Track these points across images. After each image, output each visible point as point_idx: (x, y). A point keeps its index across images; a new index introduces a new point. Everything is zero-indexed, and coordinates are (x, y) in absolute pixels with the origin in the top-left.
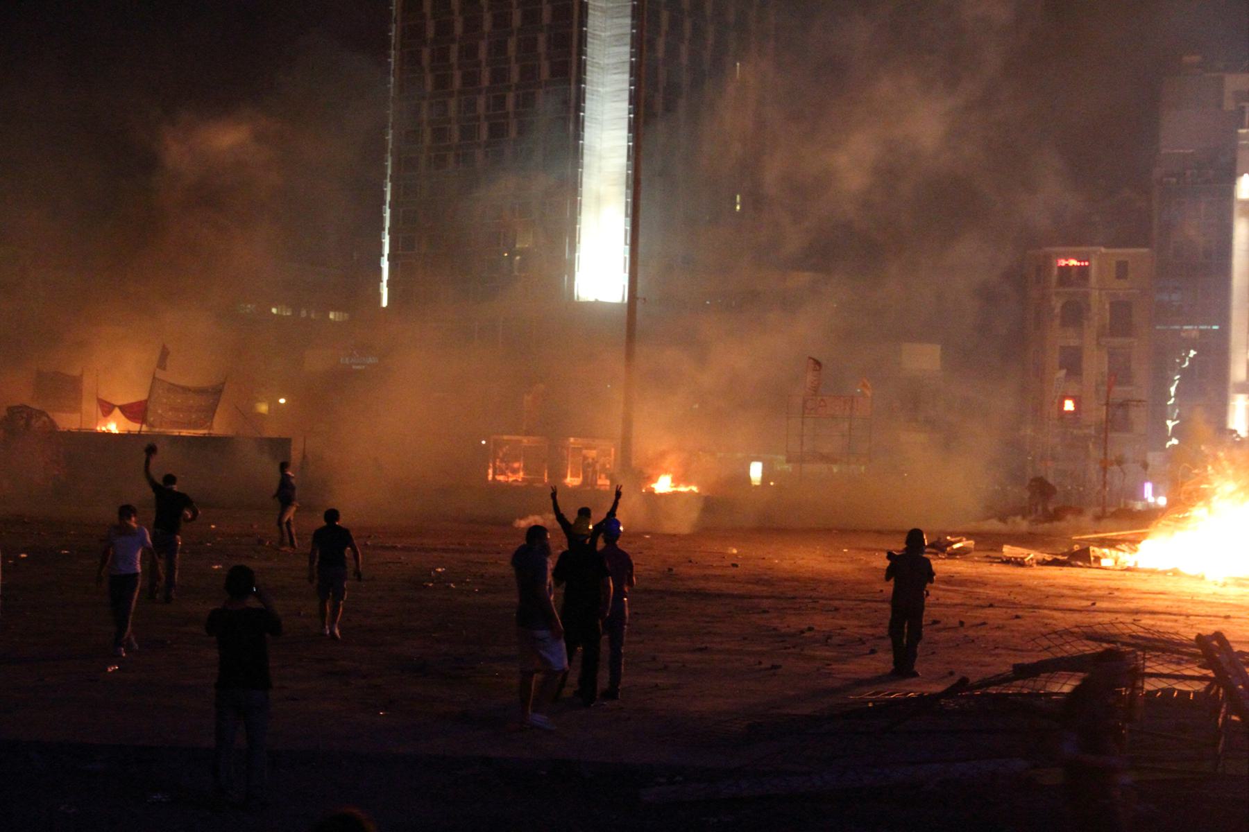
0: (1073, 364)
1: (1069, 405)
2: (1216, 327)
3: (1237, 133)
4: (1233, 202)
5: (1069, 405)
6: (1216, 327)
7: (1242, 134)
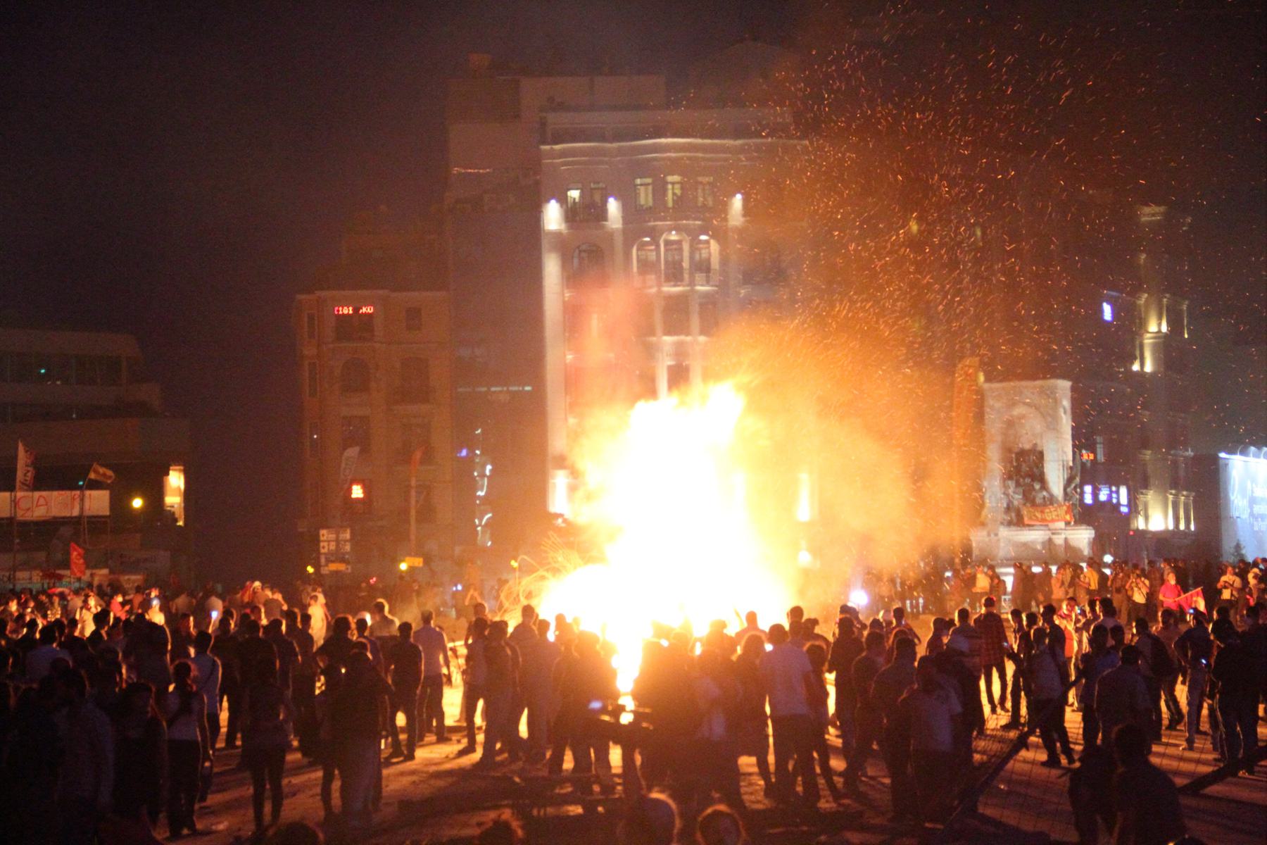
0: (359, 436)
1: (357, 492)
2: (528, 388)
3: (540, 150)
4: (540, 233)
5: (357, 492)
6: (528, 388)
7: (545, 150)
